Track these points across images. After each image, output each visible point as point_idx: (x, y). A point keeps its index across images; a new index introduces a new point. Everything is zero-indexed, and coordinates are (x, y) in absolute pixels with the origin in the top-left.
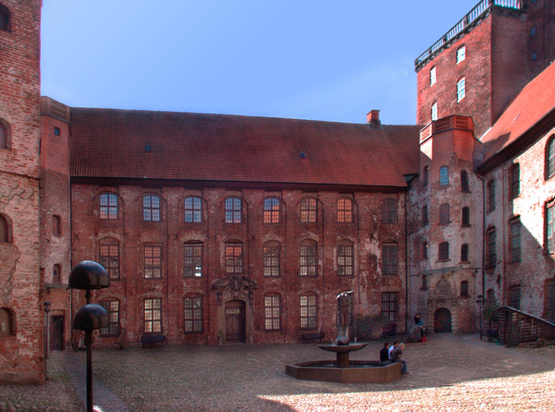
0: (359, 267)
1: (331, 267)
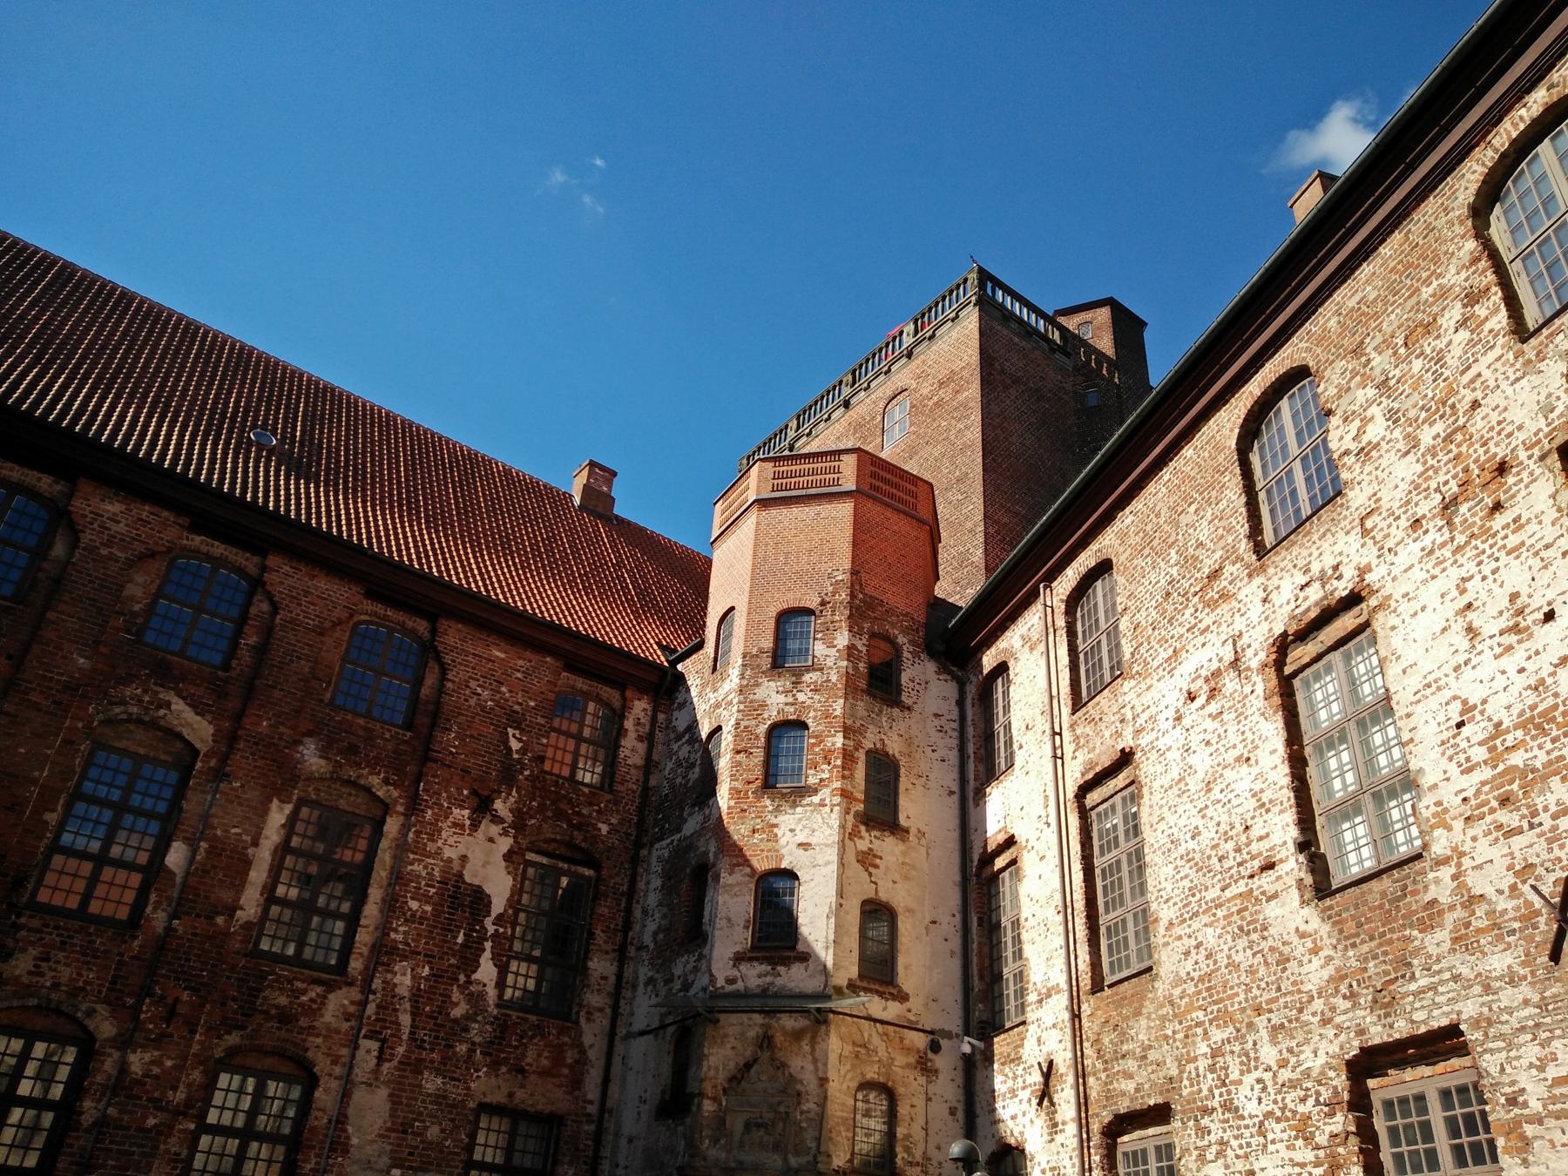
0: (385, 928)
1: (227, 896)
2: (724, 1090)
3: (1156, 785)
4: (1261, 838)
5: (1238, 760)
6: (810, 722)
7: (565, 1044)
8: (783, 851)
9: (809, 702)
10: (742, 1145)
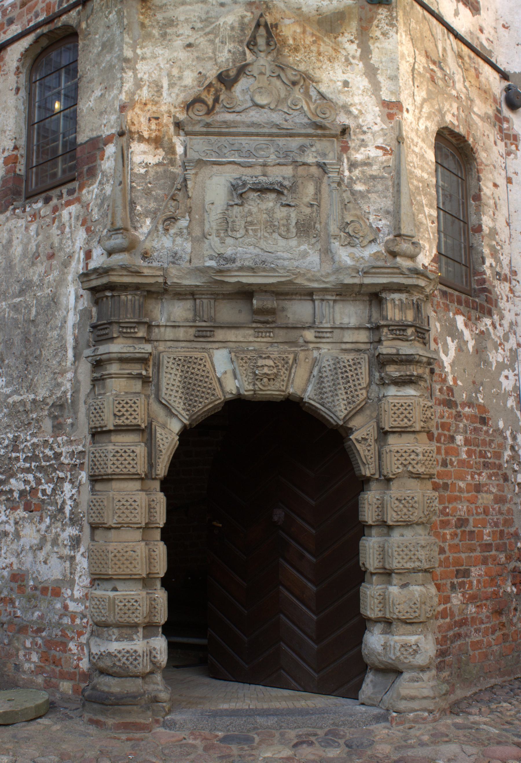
2: (178, 125)
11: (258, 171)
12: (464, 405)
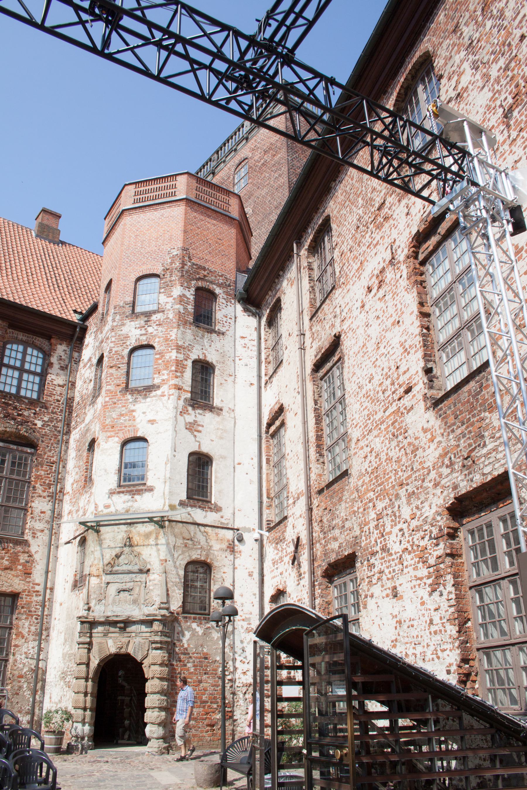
3: (351, 353)
4: (405, 373)
5: (393, 324)
6: (155, 345)
7: (19, 552)
8: (139, 426)
9: (155, 333)
10: (114, 602)
11: (124, 584)
12: (193, 653)
